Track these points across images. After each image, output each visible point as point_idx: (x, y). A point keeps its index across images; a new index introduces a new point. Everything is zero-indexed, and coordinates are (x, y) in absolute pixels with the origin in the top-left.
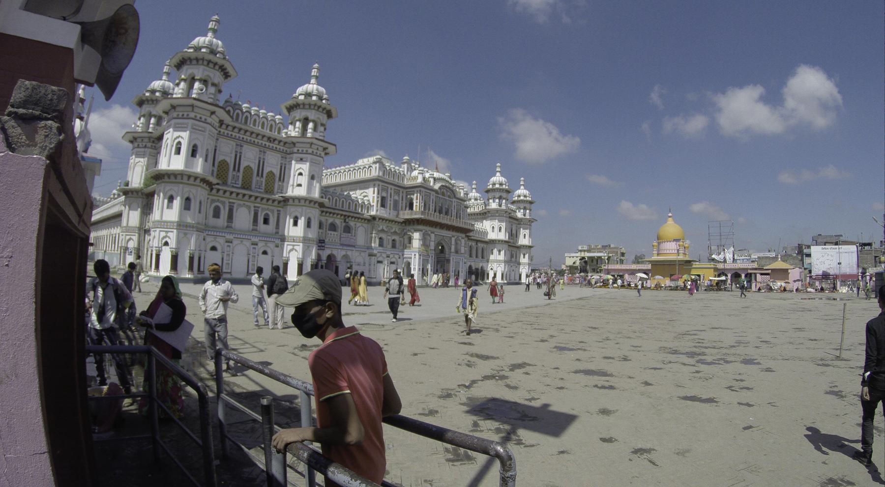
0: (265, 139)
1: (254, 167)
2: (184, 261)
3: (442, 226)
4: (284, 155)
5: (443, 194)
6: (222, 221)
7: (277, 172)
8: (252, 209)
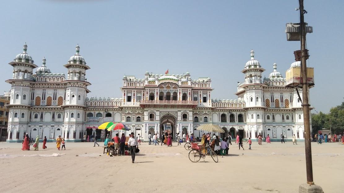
0: (55, 85)
1: (52, 97)
2: (21, 135)
3: (165, 106)
4: (65, 89)
5: (168, 87)
6: (38, 119)
7: (63, 97)
8: (52, 113)
